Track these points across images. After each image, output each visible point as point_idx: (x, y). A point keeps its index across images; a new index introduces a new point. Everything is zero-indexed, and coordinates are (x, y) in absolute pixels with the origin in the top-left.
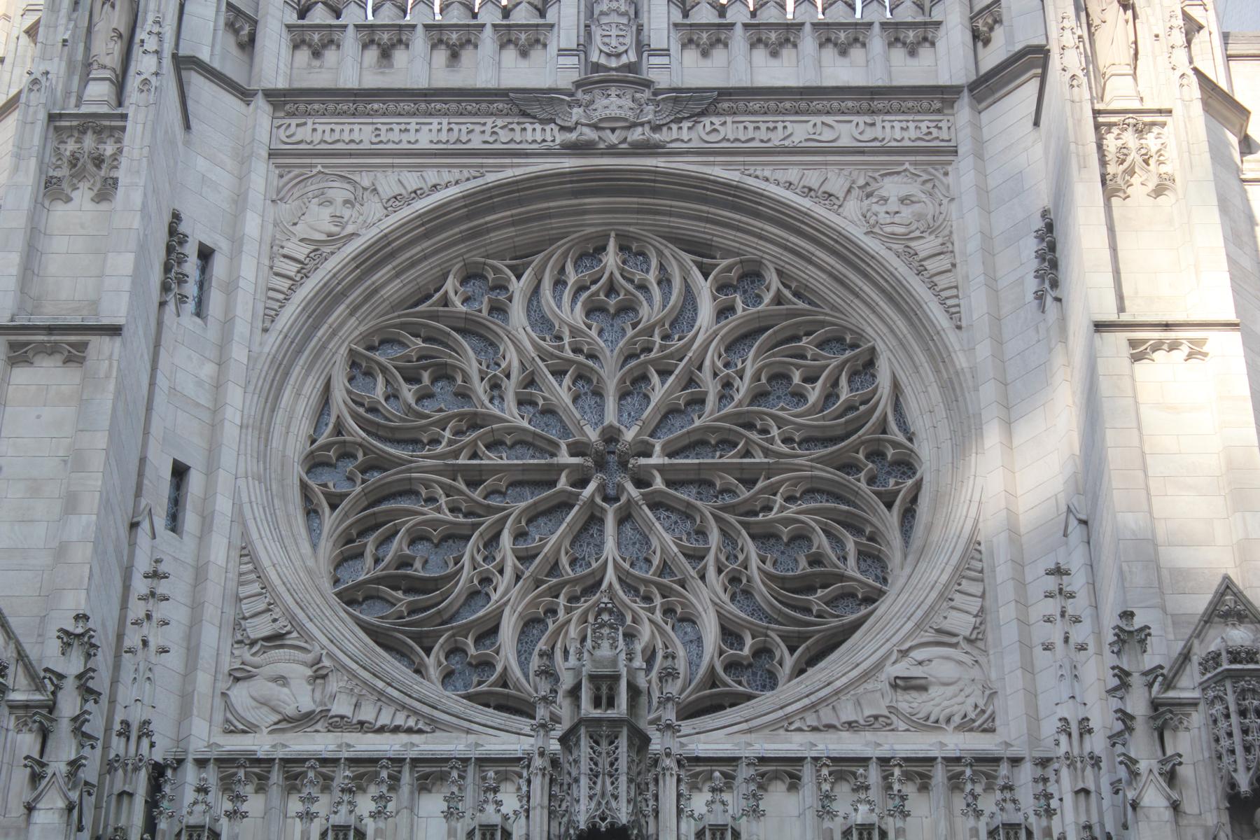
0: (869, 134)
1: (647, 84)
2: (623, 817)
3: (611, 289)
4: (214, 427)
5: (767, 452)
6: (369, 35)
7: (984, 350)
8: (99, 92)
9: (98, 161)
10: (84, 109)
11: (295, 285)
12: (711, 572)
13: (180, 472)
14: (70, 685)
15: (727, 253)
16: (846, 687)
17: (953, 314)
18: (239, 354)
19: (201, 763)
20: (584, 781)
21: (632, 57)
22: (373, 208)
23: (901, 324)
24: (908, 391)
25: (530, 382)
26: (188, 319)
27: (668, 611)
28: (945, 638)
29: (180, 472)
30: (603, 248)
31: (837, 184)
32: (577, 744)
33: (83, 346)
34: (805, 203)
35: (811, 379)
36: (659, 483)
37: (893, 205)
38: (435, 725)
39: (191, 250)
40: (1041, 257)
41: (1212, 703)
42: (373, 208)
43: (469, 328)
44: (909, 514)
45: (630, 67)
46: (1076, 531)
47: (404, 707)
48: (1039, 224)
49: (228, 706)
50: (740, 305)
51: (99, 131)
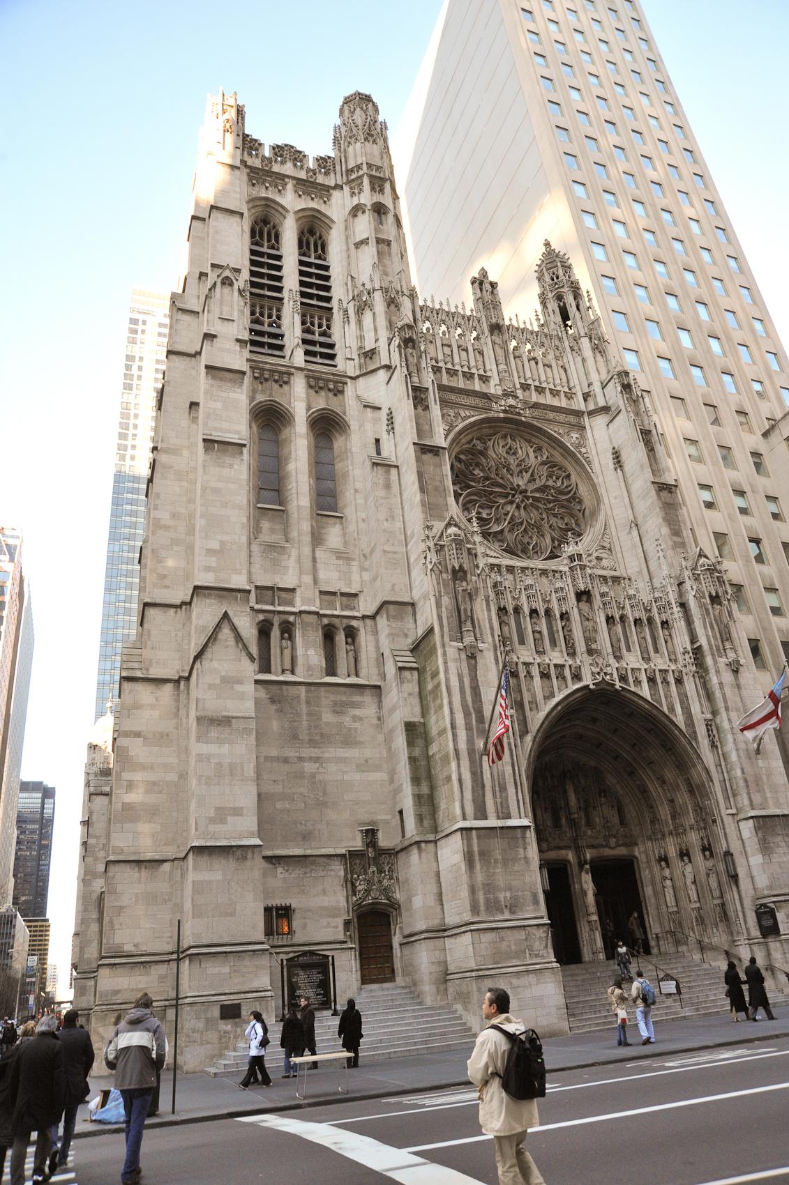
1: (517, 397)
3: (510, 448)
5: (553, 496)
6: (480, 377)
9: (422, 399)
15: (534, 443)
22: (460, 420)
23: (578, 468)
24: (580, 486)
25: (496, 470)
27: (538, 532)
32: (576, 570)
33: (438, 451)
34: (556, 435)
36: (531, 501)
37: (574, 439)
42: (460, 420)
44: (583, 514)
45: (513, 392)
46: (634, 529)
50: (539, 458)
51: (420, 391)
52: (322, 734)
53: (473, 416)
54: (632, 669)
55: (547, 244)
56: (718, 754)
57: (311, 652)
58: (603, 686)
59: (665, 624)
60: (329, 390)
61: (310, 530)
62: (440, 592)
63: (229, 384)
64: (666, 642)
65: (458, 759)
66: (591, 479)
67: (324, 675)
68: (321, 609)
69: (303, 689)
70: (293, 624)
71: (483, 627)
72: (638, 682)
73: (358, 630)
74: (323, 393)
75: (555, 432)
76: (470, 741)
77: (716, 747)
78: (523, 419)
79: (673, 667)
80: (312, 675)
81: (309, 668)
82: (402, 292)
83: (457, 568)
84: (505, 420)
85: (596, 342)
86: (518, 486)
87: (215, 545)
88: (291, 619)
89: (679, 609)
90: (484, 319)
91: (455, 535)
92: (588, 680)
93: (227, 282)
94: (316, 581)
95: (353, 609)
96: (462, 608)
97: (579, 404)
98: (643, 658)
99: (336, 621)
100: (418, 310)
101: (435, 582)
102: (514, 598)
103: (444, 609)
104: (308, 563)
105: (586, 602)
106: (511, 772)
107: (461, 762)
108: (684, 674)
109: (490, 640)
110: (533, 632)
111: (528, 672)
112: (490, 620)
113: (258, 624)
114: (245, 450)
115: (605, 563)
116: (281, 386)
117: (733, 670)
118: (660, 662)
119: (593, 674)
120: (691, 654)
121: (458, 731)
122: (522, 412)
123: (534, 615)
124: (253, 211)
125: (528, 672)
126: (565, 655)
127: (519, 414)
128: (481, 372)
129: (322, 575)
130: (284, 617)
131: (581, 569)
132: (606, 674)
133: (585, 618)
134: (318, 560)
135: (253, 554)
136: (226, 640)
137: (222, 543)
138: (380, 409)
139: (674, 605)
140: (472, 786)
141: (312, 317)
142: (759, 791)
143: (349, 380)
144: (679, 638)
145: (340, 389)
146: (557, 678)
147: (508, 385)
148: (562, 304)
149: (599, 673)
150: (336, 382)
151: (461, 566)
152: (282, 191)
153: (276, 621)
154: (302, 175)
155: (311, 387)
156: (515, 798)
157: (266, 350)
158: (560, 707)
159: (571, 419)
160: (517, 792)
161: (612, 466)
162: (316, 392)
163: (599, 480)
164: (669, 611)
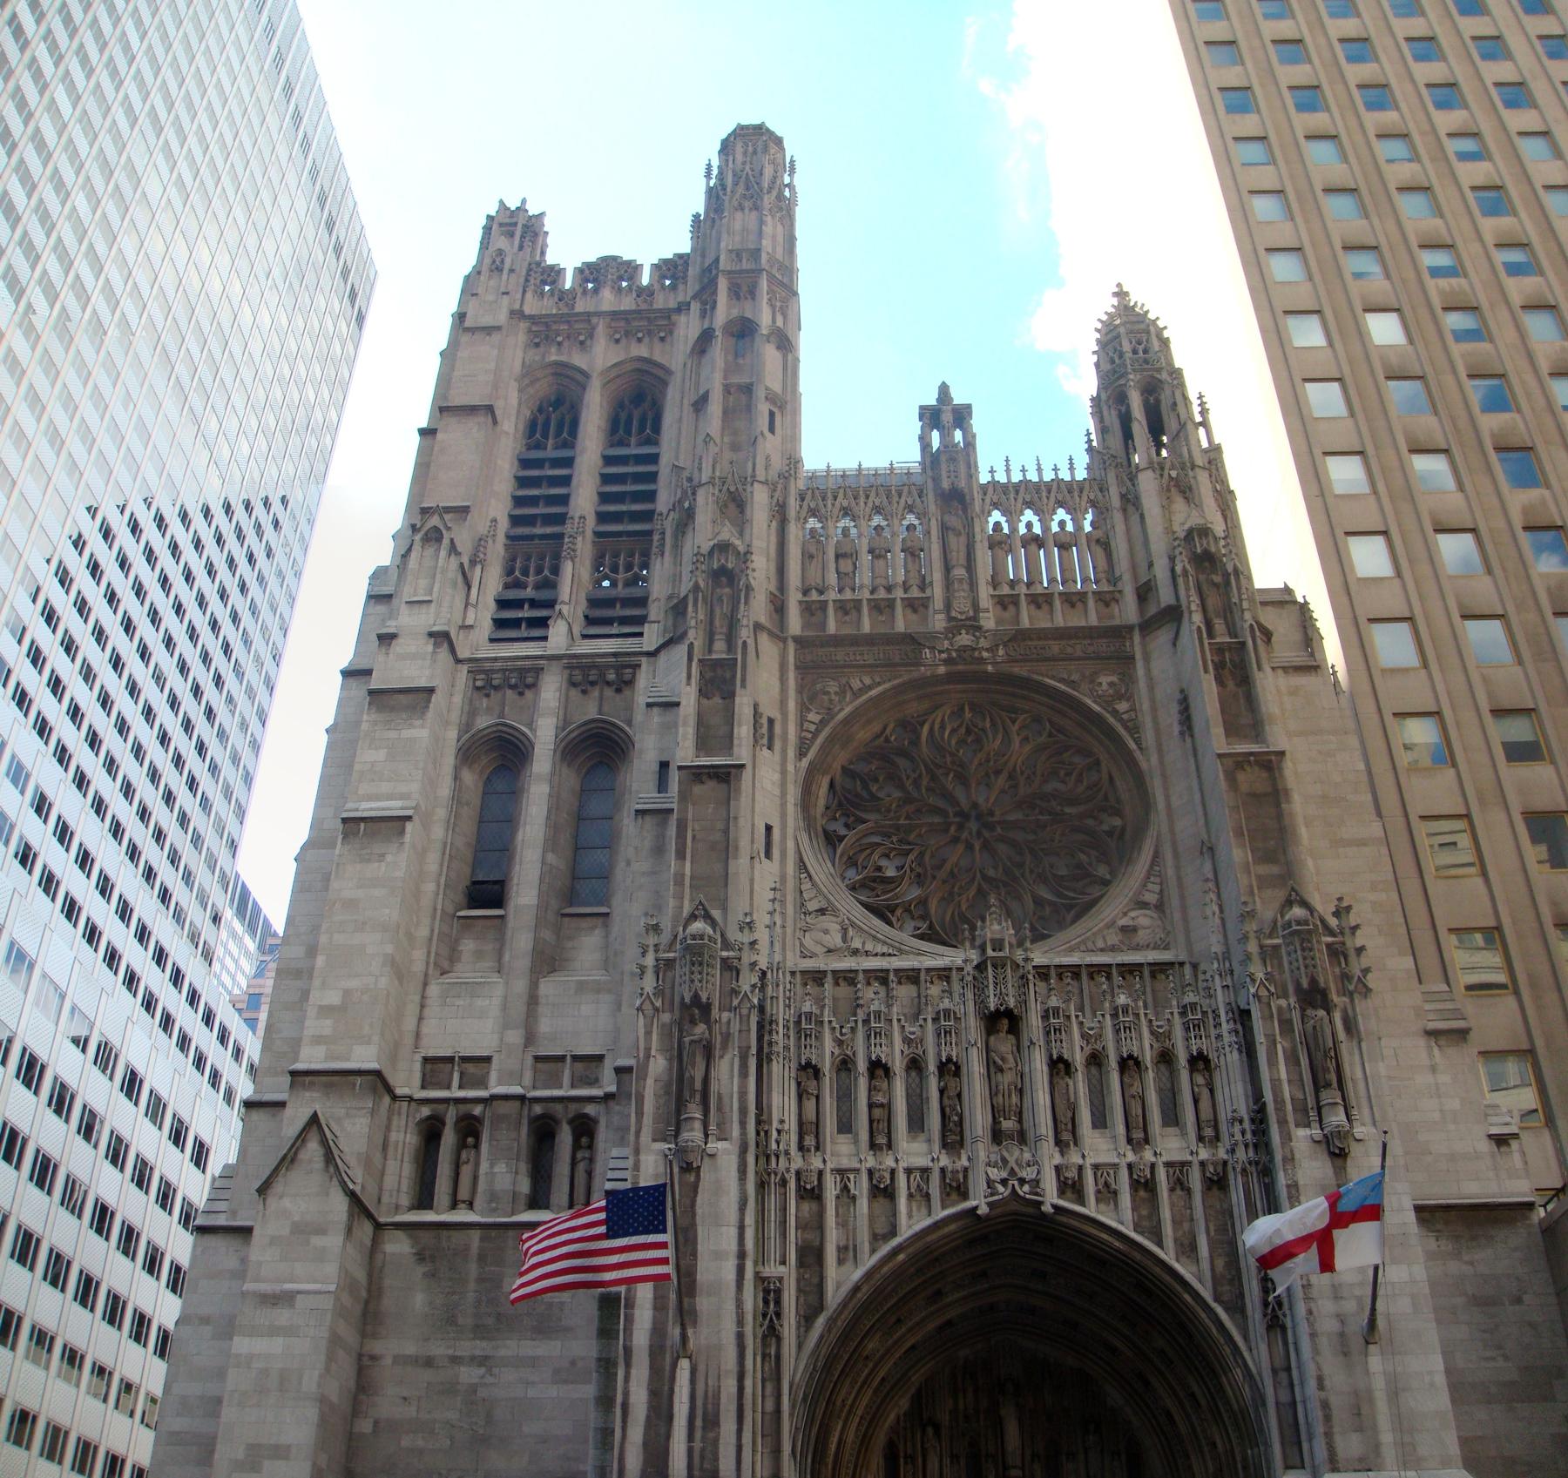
0: (1091, 649)
1: (979, 628)
2: (1012, 1003)
4: (783, 805)
7: (1154, 759)
8: (720, 645)
10: (714, 656)
11: (815, 735)
12: (1027, 874)
13: (769, 828)
14: (746, 948)
16: (1100, 930)
17: (1138, 742)
18: (790, 768)
19: (793, 973)
20: (991, 987)
21: (971, 613)
26: (766, 752)
28: (1144, 905)
29: (769, 828)
30: (962, 709)
31: (1075, 677)
34: (1062, 687)
35: (1068, 774)
37: (1105, 686)
38: (901, 952)
39: (764, 721)
40: (1181, 713)
41: (1287, 945)
43: (903, 753)
47: (885, 943)
48: (1178, 696)
49: (801, 944)
52: (499, 1317)
53: (879, 684)
54: (1096, 1167)
55: (1121, 294)
56: (1286, 1343)
57: (501, 1168)
58: (1014, 1206)
59: (1200, 1062)
60: (608, 684)
61: (530, 946)
62: (648, 1049)
63: (404, 716)
64: (1196, 1101)
65: (628, 1365)
66: (1132, 763)
67: (522, 1207)
68: (534, 1088)
69: (476, 1235)
70: (479, 1120)
71: (727, 1109)
72: (1108, 1194)
73: (595, 1121)
74: (596, 693)
75: (1062, 680)
76: (658, 1331)
77: (1283, 1328)
78: (990, 668)
79: (1204, 1154)
80: (494, 1210)
81: (493, 1197)
82: (754, 476)
83: (687, 1000)
84: (951, 678)
85: (1174, 474)
86: (975, 805)
87: (333, 998)
88: (477, 1110)
89: (1232, 1025)
90: (930, 484)
91: (694, 937)
92: (978, 1201)
93: (434, 537)
94: (530, 1039)
95: (594, 1082)
96: (687, 1075)
97: (1129, 612)
98: (1130, 1141)
99: (558, 1108)
100: (793, 503)
101: (641, 1031)
102: (840, 1043)
103: (650, 1082)
104: (518, 1008)
105: (1009, 1032)
106: (734, 1390)
107: (633, 1372)
108: (1230, 1168)
109: (736, 1132)
110: (871, 1106)
111: (845, 1189)
112: (743, 1094)
113: (418, 1124)
114: (409, 826)
115: (1142, 937)
116: (521, 694)
117: (1332, 1155)
118: (1171, 1146)
119: (990, 1183)
120: (1247, 1125)
121: (637, 1312)
122: (985, 654)
123: (880, 1072)
124: (531, 391)
125: (845, 1189)
126: (937, 1146)
127: (981, 660)
128: (915, 593)
129: (544, 1026)
130: (463, 1108)
131: (995, 966)
132: (1022, 1181)
133: (993, 1067)
134: (542, 1000)
135: (429, 1002)
136: (310, 1161)
137: (347, 993)
138: (678, 704)
139: (1223, 1018)
140: (648, 1418)
141: (616, 555)
142: (1360, 1429)
143: (644, 660)
144: (1226, 1090)
145: (627, 677)
146: (910, 1196)
147: (962, 605)
148: (1123, 409)
149: (1004, 1182)
150: (620, 668)
151: (696, 997)
152: (588, 342)
153: (451, 1116)
154: (628, 303)
155: (573, 684)
156: (733, 1440)
157: (524, 632)
158: (901, 1257)
159: (1102, 646)
160: (740, 1431)
161: (1176, 729)
162: (584, 692)
163: (1148, 762)
164: (1213, 1032)
